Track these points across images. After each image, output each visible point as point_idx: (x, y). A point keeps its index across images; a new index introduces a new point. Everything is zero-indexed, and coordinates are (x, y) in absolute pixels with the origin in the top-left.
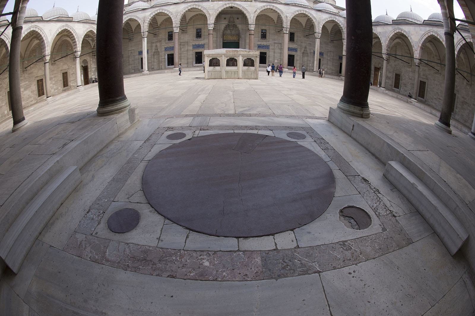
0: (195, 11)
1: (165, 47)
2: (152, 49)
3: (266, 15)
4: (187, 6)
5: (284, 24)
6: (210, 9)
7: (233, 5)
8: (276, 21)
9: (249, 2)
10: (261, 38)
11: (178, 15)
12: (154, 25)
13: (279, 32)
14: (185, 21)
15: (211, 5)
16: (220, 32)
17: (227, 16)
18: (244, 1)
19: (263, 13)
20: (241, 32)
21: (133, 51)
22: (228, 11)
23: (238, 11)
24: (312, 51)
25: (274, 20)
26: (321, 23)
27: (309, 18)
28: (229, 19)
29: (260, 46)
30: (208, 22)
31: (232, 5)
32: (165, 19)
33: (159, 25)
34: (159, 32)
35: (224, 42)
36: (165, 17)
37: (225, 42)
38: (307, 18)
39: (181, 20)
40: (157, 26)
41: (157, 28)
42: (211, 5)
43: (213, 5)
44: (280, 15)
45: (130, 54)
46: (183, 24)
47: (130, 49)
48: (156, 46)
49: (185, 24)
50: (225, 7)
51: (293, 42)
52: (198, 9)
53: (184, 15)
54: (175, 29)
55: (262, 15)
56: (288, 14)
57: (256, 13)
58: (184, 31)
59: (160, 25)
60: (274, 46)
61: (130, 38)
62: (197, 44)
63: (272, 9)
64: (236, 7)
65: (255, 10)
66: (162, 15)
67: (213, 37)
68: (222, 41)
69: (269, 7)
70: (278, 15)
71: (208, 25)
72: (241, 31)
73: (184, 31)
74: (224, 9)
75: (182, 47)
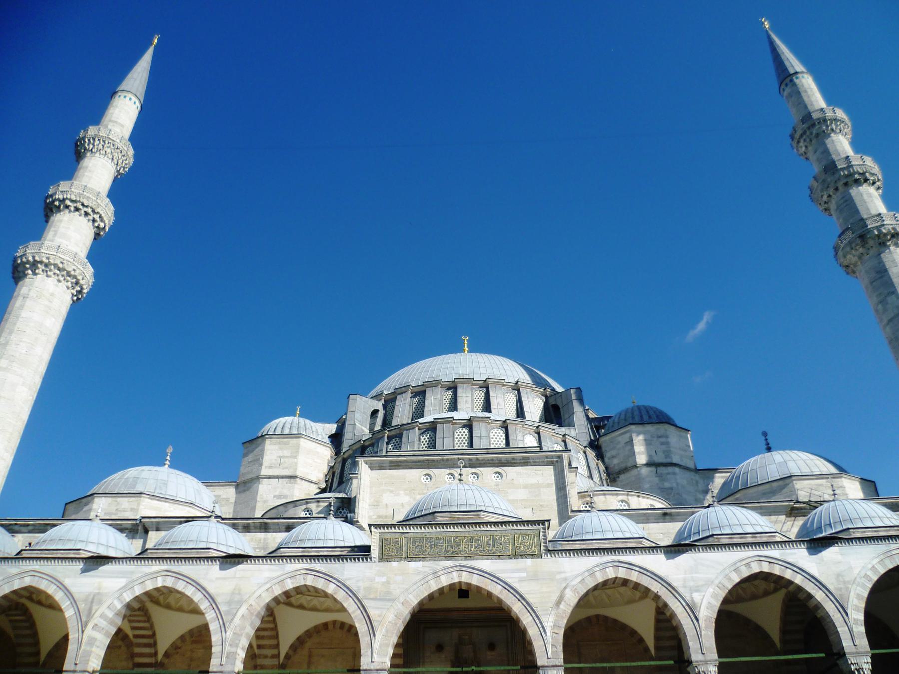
0: (319, 607)
3: (606, 618)
4: (278, 573)
5: (690, 643)
6: (372, 596)
7: (466, 578)
8: (650, 642)
9: (529, 561)
11: (239, 614)
12: (137, 650)
14: (275, 651)
15: (377, 579)
17: (450, 636)
18: (510, 557)
19: (591, 612)
22: (449, 610)
25: (641, 640)
26: (852, 595)
27: (791, 588)
31: (463, 580)
32: (191, 632)
33: (160, 656)
36: (192, 622)
38: (781, 595)
39: (259, 646)
42: (377, 579)
43: (384, 579)
44: (666, 605)
49: (272, 667)
50: (434, 586)
52: (326, 595)
53: (268, 622)
55: (589, 619)
56: (697, 591)
57: (562, 606)
59: (167, 654)
63: (625, 582)
64: (479, 589)
65: (558, 594)
66: (180, 609)
69: (611, 573)
74: (431, 597)
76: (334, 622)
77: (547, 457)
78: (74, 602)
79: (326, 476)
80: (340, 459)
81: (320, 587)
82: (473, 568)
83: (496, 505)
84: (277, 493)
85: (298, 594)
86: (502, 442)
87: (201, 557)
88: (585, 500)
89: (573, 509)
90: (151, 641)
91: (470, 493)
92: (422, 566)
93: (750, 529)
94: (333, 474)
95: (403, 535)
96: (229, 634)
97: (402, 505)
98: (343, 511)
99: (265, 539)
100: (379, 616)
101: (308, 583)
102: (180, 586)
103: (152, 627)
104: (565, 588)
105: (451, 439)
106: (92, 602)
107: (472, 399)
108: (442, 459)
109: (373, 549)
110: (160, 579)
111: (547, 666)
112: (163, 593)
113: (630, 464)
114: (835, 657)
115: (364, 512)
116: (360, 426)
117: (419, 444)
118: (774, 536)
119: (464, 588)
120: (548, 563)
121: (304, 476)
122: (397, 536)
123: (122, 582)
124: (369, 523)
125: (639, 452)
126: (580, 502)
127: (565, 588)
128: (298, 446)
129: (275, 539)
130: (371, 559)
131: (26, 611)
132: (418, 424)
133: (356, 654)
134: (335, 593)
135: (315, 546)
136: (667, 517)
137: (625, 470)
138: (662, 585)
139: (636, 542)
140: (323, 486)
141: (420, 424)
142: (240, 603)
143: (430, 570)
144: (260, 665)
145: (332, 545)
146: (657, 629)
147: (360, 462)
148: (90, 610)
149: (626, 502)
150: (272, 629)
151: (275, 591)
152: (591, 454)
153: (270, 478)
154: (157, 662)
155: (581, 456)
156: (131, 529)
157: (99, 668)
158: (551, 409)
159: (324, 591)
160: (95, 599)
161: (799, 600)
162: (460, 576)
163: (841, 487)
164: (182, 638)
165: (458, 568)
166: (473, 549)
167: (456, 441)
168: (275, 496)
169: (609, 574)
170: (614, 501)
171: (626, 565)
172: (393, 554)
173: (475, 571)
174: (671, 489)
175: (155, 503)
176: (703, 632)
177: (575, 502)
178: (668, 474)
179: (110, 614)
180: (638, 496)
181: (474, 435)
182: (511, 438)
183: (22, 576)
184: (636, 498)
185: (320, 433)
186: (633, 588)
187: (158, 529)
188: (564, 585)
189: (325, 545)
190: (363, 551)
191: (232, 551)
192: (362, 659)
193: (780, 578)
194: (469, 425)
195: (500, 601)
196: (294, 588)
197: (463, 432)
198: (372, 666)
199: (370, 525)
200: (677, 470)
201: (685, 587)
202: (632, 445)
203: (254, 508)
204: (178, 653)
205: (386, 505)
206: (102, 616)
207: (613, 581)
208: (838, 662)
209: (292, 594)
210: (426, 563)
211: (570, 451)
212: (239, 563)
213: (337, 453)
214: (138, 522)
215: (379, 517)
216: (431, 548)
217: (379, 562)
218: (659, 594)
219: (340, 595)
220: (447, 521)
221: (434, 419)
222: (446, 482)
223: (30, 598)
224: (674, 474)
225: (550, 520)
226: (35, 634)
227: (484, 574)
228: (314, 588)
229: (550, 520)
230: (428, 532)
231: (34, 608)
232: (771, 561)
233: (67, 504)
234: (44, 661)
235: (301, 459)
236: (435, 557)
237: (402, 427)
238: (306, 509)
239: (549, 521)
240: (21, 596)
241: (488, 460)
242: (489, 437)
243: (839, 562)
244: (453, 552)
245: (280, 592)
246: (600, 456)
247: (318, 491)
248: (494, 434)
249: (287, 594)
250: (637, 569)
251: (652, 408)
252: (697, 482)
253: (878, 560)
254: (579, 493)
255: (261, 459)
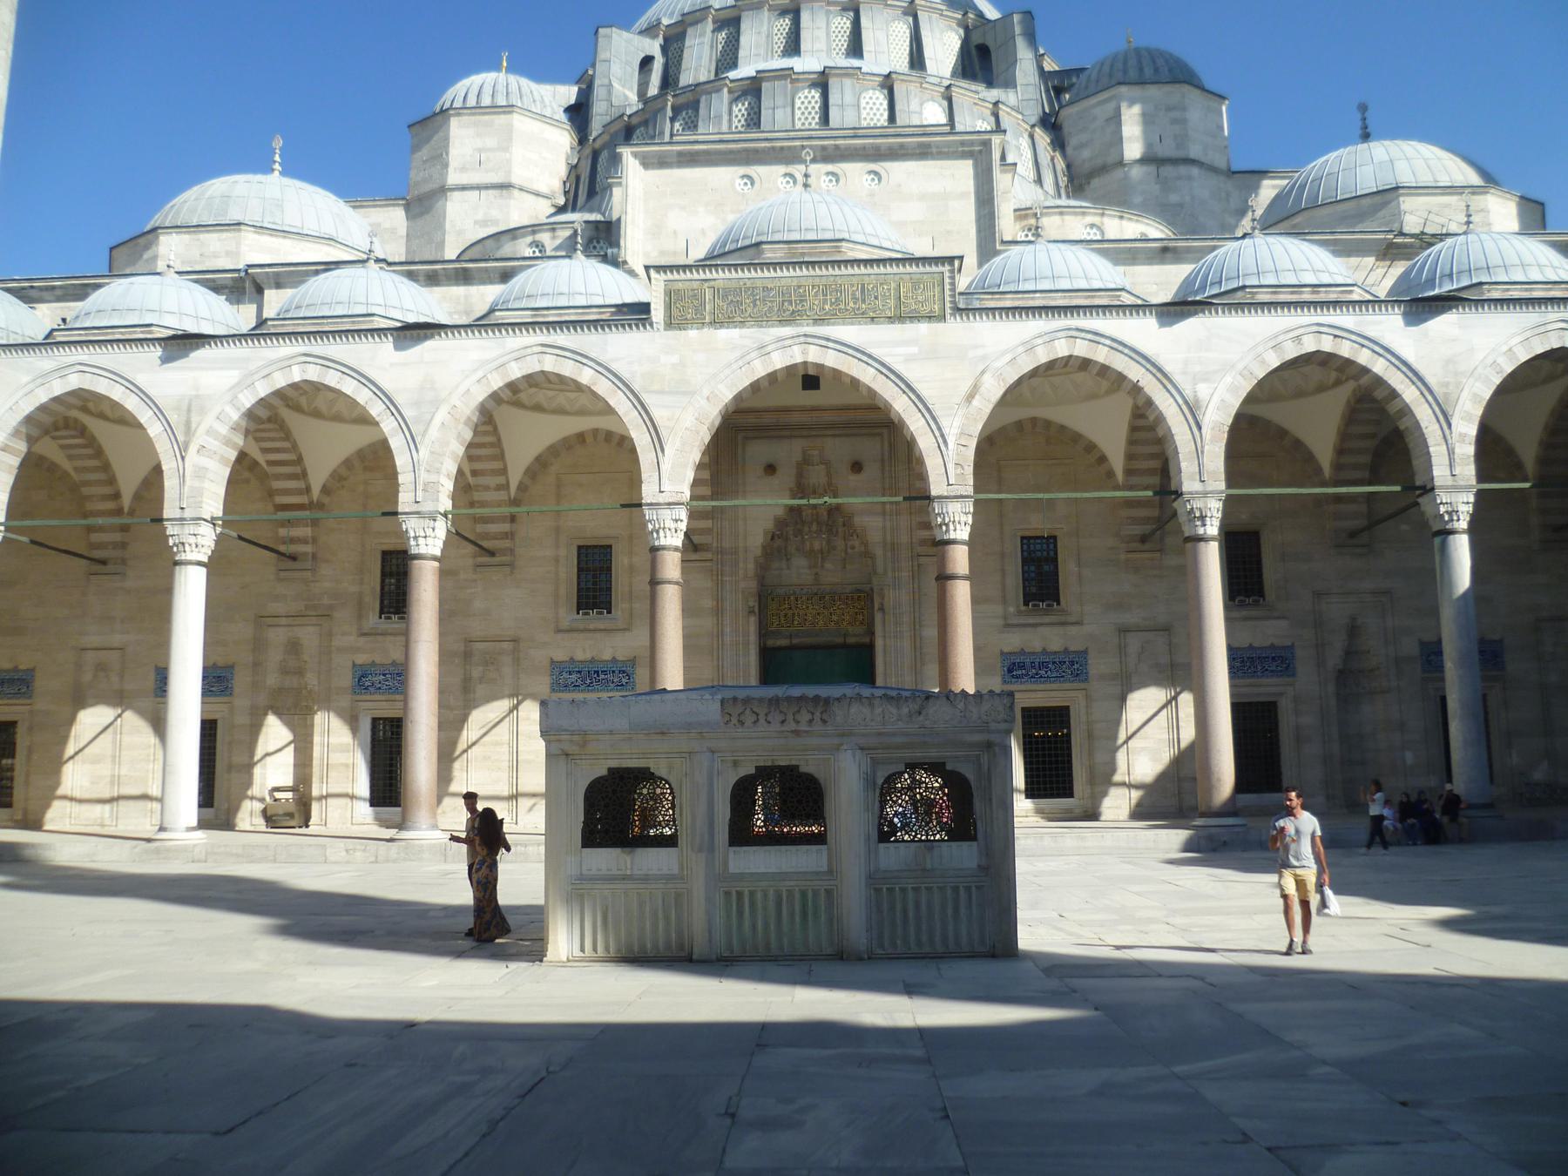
1: (354, 665)
2: (256, 664)
3: (1048, 424)
5: (1183, 465)
7: (814, 355)
8: (1117, 463)
9: (923, 328)
10: (1026, 603)
11: (437, 421)
12: (277, 485)
13: (1144, 539)
14: (501, 480)
16: (741, 572)
17: (787, 452)
18: (891, 320)
20: (880, 570)
21: (115, 655)
22: (787, 410)
23: (856, 408)
24: (1410, 647)
25: (1103, 459)
26: (1465, 394)
27: (1364, 380)
28: (800, 475)
29: (1022, 666)
30: (649, 492)
32: (360, 454)
34: (314, 540)
35: (770, 643)
37: (780, 648)
38: (1344, 393)
39: (474, 473)
40: (299, 492)
41: (301, 507)
43: (675, 359)
44: (1149, 403)
45: (87, 677)
46: (483, 504)
47: (94, 640)
48: (294, 647)
50: (760, 370)
51: (1256, 603)
52: (578, 387)
54: (411, 525)
55: (1019, 425)
56: (1205, 380)
57: (975, 402)
58: (492, 553)
59: (325, 490)
60: (1122, 650)
61: (97, 554)
62: (580, 656)
63: (1085, 363)
64: (837, 374)
66: (337, 418)
67: (688, 610)
68: (753, 638)
69: (1062, 349)
70: (1136, 407)
71: (648, 513)
72: (880, 563)
73: (492, 553)
74: (755, 387)
75: (476, 672)
76: (595, 432)
77: (963, 143)
78: (159, 412)
79: (564, 183)
80: (588, 151)
81: (567, 375)
82: (828, 340)
83: (869, 230)
84: (480, 216)
85: (531, 386)
86: (882, 115)
87: (358, 329)
88: (1025, 223)
89: (1006, 238)
90: (298, 470)
91: (822, 209)
92: (741, 337)
93: (1310, 279)
94: (578, 178)
95: (706, 285)
96: (424, 453)
97: (703, 232)
98: (598, 246)
99: (466, 297)
100: (668, 419)
101: (548, 368)
102: (332, 379)
103: (295, 447)
104: (983, 372)
105: (789, 110)
106: (189, 410)
107: (828, 34)
108: (773, 148)
109: (656, 309)
110: (295, 368)
111: (946, 497)
112: (305, 393)
113: (1111, 159)
114: (1418, 492)
115: (636, 245)
116: (621, 88)
117: (730, 121)
118: (1351, 292)
119: (811, 372)
120: (955, 329)
121: (526, 185)
122: (695, 285)
123: (233, 376)
124: (648, 264)
125: (1130, 138)
126: (1018, 227)
127: (983, 372)
128: (509, 130)
129: (483, 296)
130: (651, 325)
131: (82, 431)
132: (728, 82)
133: (635, 481)
134: (595, 384)
135: (554, 305)
136: (1169, 255)
137: (1103, 169)
138: (1148, 370)
139: (1109, 296)
140: (561, 201)
141: (732, 81)
142: (436, 403)
143: (754, 343)
144: (478, 502)
145: (584, 304)
146: (1131, 442)
147: (625, 154)
148: (188, 424)
149: (1099, 228)
150: (492, 445)
151: (492, 383)
152: (1043, 139)
153: (464, 188)
154: (311, 503)
155: (1024, 142)
156: (233, 287)
157: (220, 514)
158: (974, 52)
159: (575, 381)
160: (192, 406)
161: (1374, 400)
162: (804, 353)
163: (1482, 210)
164: (347, 463)
165: (802, 339)
166: (827, 307)
167: (798, 113)
168: (476, 222)
169: (1059, 349)
170: (1077, 226)
171: (1089, 336)
172: (689, 316)
173: (831, 345)
174: (1181, 205)
175: (266, 240)
176: (1206, 448)
177: (1007, 226)
178: (1179, 178)
179: (224, 430)
180: (1121, 217)
181: (831, 101)
182: (898, 108)
183: (61, 371)
184: (1116, 221)
185: (548, 103)
186: (1098, 374)
187: (278, 286)
188: (981, 368)
189: (571, 304)
190: (637, 313)
191: (411, 319)
192: (644, 487)
193: (1349, 363)
194: (822, 82)
195: (872, 393)
196: (523, 377)
197: (810, 96)
198: (661, 499)
199: (647, 268)
200: (1195, 171)
201: (1184, 373)
202: (1119, 124)
203: (441, 244)
204: (343, 487)
205: (675, 232)
206: (210, 432)
207: (1064, 361)
208: (1420, 500)
209: (522, 388)
210: (745, 331)
211: (1005, 131)
212: (426, 338)
213: (582, 139)
214: (243, 274)
215: (662, 253)
216: (755, 305)
217: (665, 330)
218: (1140, 384)
219: (603, 387)
220: (781, 257)
221: (758, 72)
222: (779, 190)
223: (85, 409)
224: (1190, 178)
225: (962, 257)
226: (106, 467)
227: (845, 349)
228: (558, 375)
229: (962, 257)
230: (749, 279)
231: (94, 425)
232: (1339, 333)
233: (111, 249)
234: (130, 508)
235: (518, 152)
236: (761, 321)
237: (697, 89)
238: (534, 241)
239: (961, 258)
240: (70, 406)
241: (856, 149)
242: (859, 106)
243: (1453, 340)
244: (793, 311)
245: (501, 384)
246: (1059, 143)
247: (552, 210)
248: (867, 100)
249: (512, 386)
250: (1108, 342)
251: (1161, 53)
252: (1228, 195)
253: (1520, 338)
254: (1015, 210)
255: (444, 156)
